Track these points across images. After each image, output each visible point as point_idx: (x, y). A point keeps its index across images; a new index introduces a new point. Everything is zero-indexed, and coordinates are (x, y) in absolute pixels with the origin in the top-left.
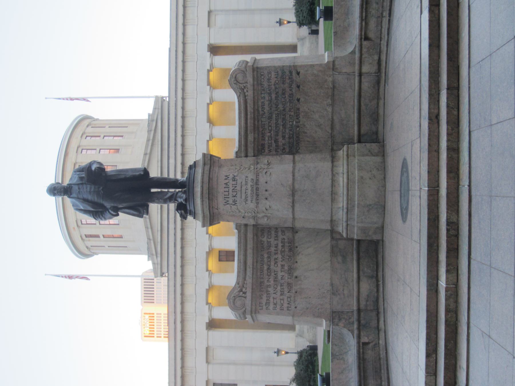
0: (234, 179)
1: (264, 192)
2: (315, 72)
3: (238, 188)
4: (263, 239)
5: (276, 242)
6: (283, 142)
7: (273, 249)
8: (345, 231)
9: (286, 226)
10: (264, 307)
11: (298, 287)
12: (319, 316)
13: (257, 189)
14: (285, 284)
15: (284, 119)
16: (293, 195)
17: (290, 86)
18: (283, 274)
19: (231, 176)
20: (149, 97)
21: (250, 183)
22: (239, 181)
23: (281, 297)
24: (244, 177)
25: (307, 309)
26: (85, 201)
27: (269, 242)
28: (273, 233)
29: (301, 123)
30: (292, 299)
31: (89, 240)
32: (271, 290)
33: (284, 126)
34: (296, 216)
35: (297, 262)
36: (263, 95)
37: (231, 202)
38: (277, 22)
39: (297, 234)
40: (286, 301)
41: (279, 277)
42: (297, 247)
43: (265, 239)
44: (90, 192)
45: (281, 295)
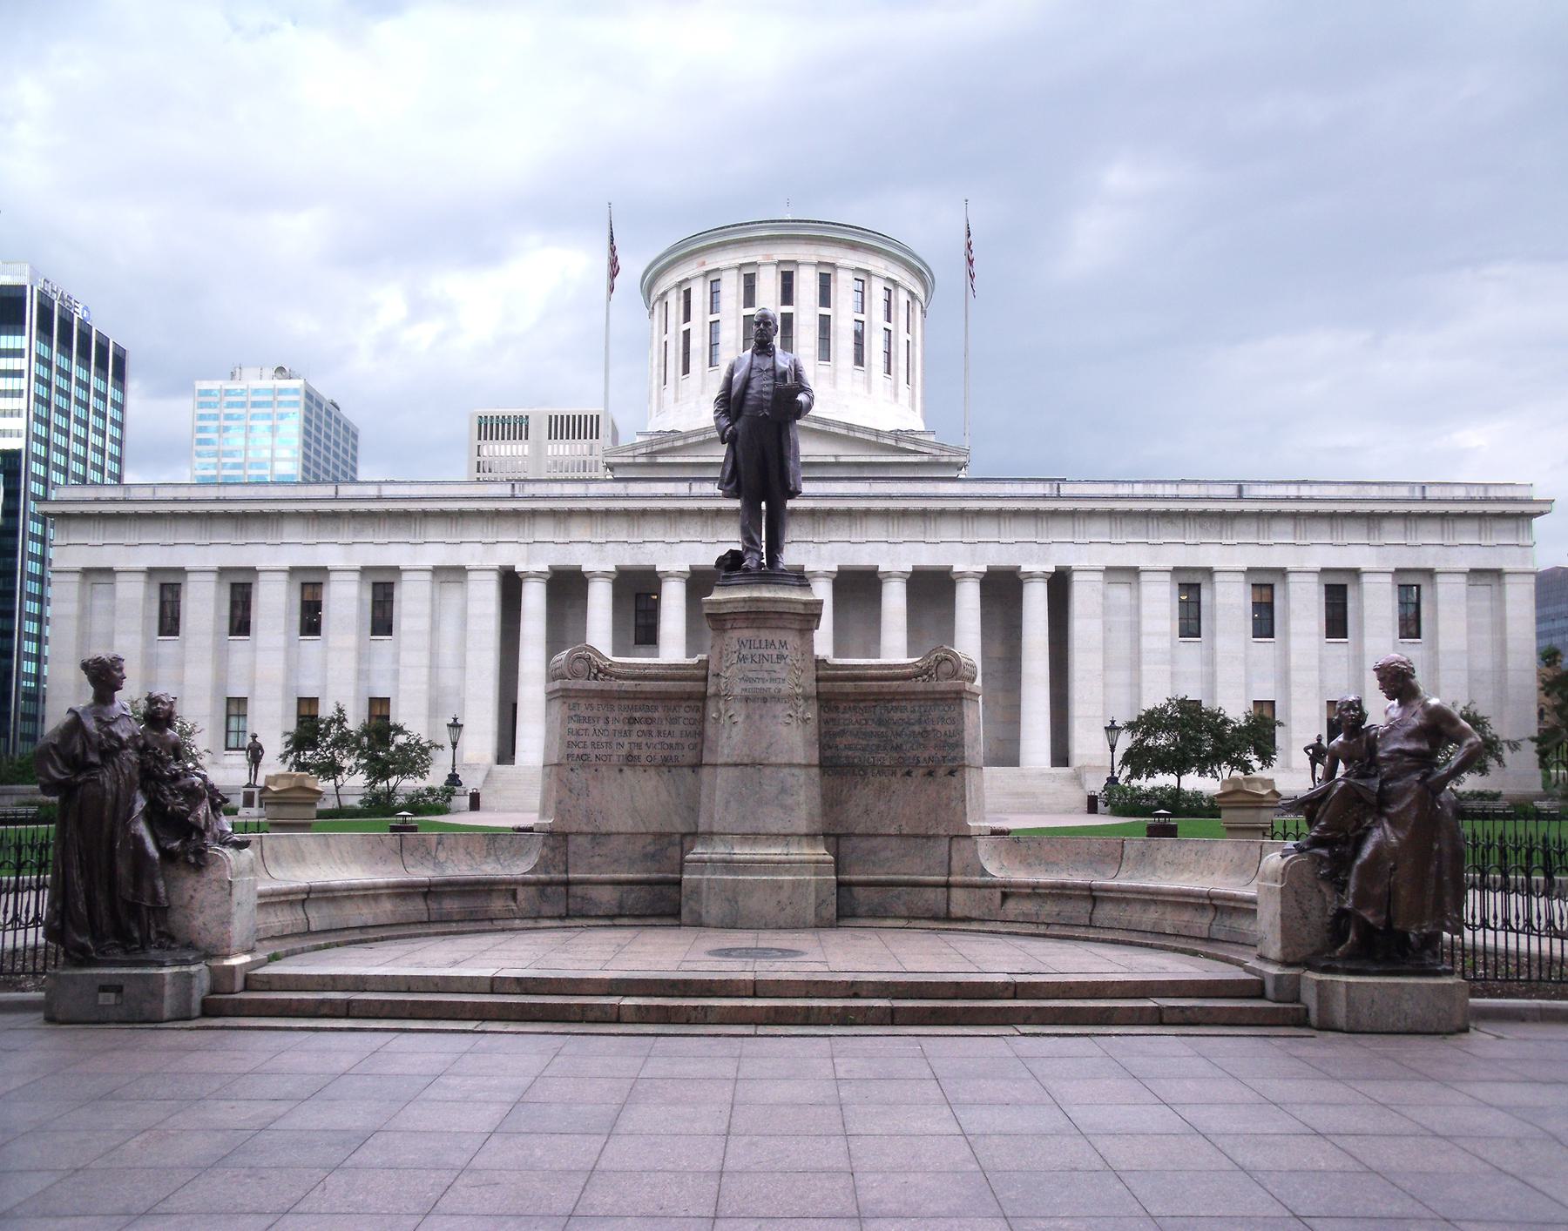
5: (677, 733)
9: (705, 752)
12: (560, 813)
16: (753, 765)
18: (627, 746)
26: (747, 382)
32: (600, 725)
34: (719, 770)
40: (581, 751)
43: (682, 713)
44: (761, 392)
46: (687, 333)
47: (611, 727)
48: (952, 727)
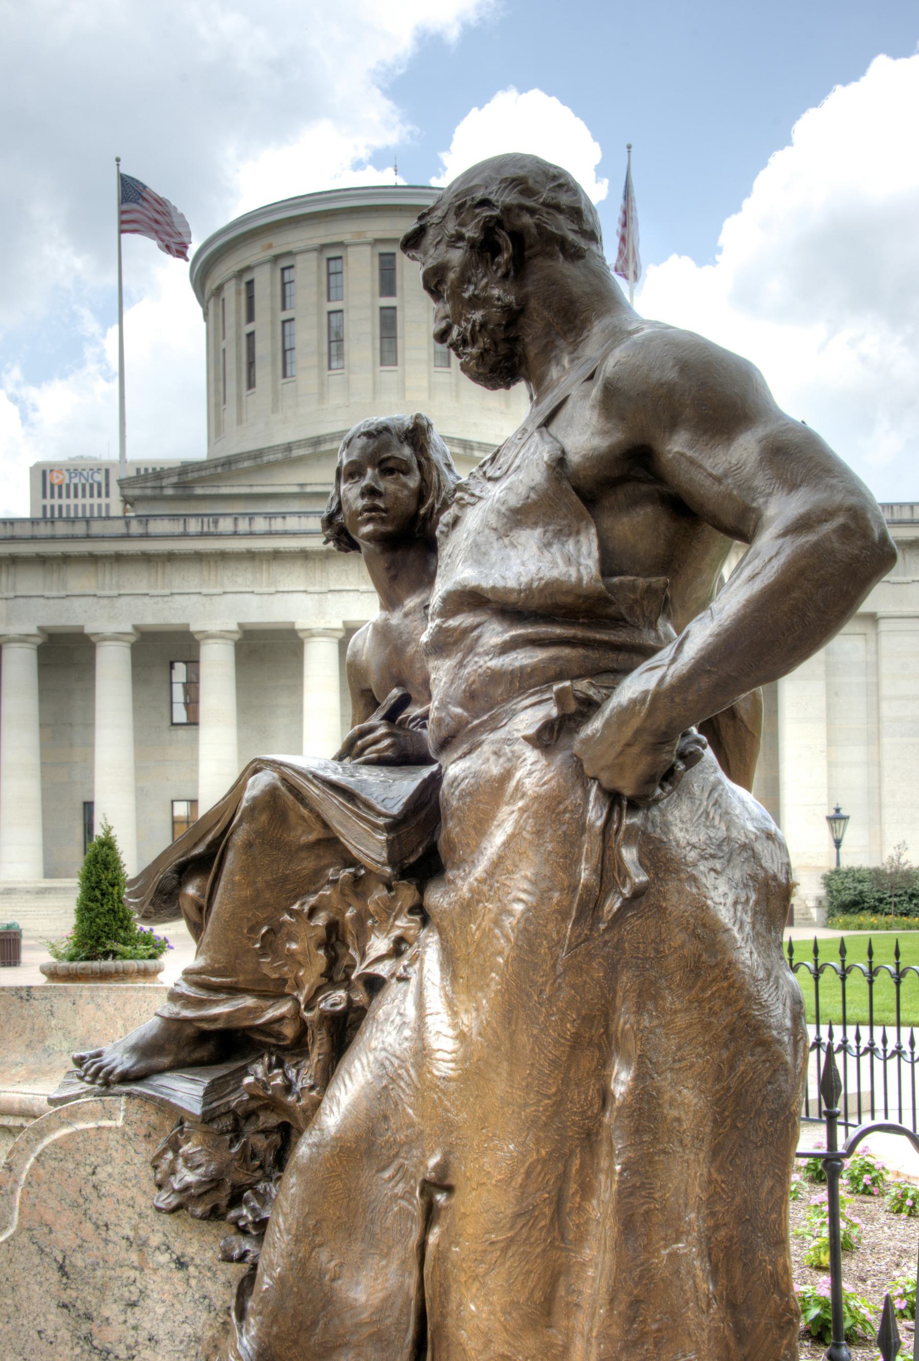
31: (238, 293)
38: (838, 810)
46: (251, 336)
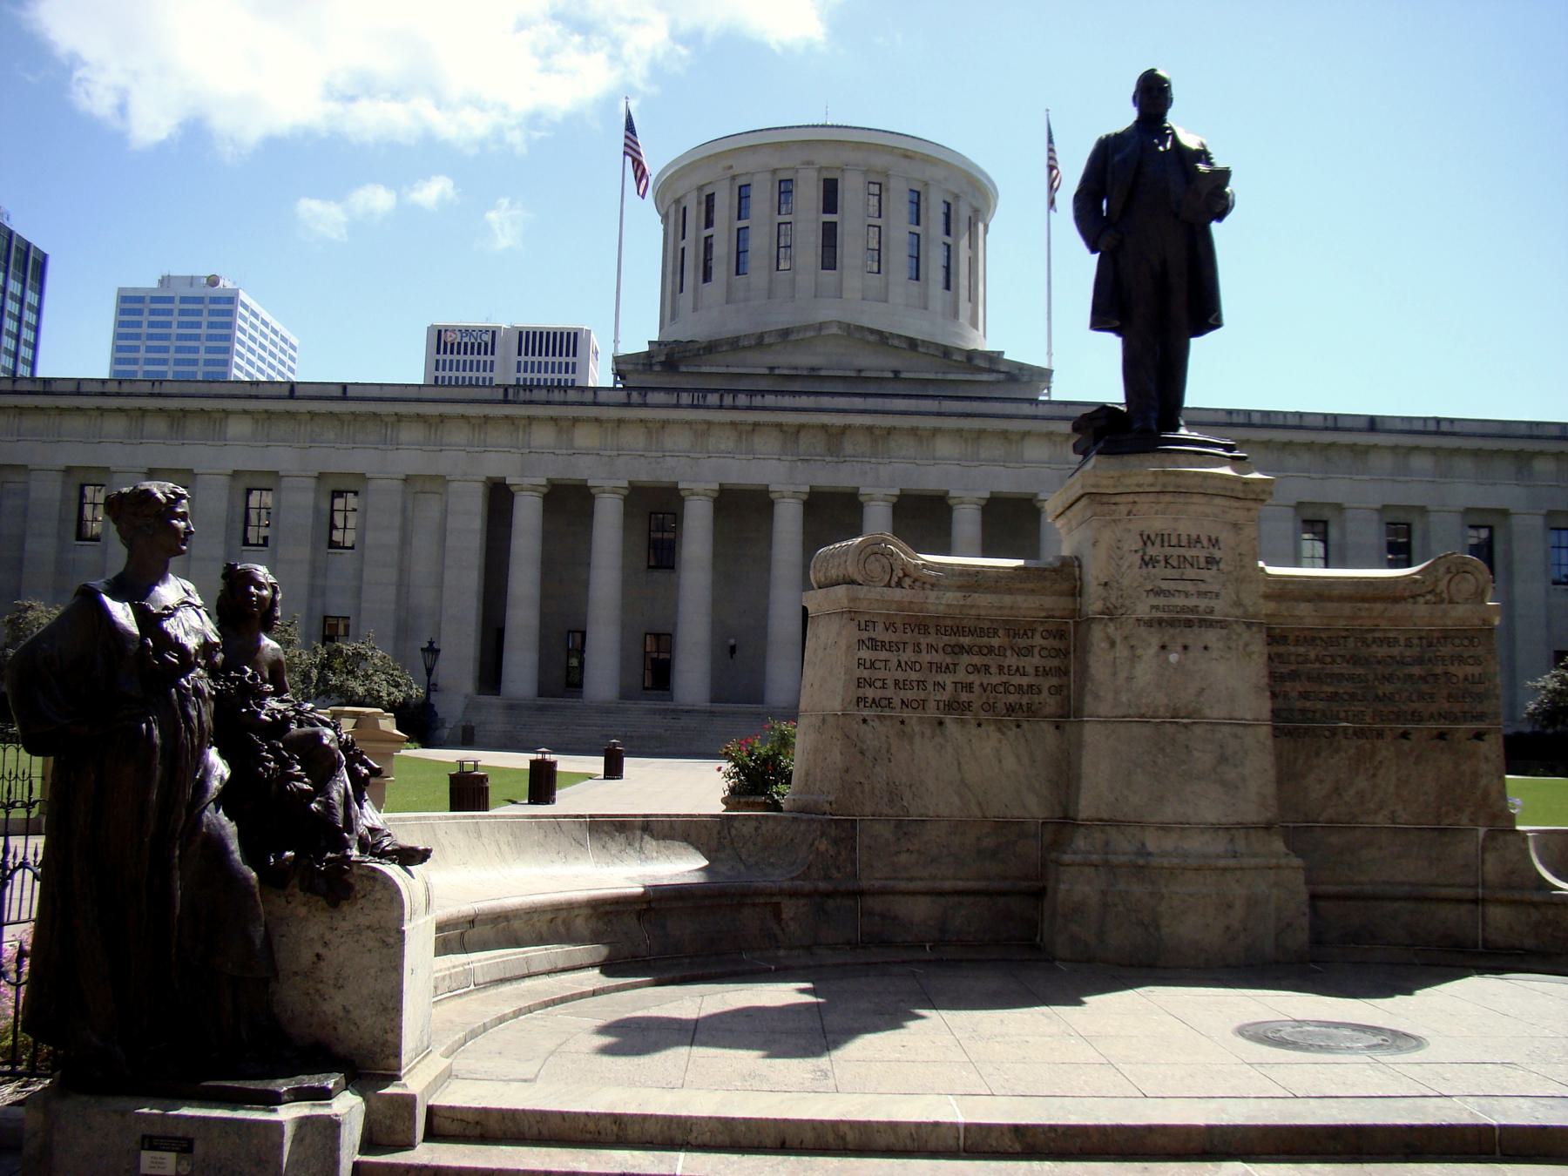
0: (1211, 561)
1: (1180, 641)
2: (1483, 782)
3: (1190, 573)
4: (1038, 636)
6: (1294, 694)
7: (1012, 660)
8: (1079, 858)
9: (1088, 699)
10: (865, 635)
11: (917, 729)
13: (1189, 624)
14: (923, 695)
15: (1353, 696)
17: (1442, 716)
18: (950, 687)
19: (1217, 554)
20: (1050, 354)
21: (1203, 603)
22: (1205, 574)
23: (890, 683)
24: (1216, 588)
25: (862, 753)
27: (1029, 651)
28: (1056, 663)
29: (1344, 742)
30: (887, 713)
31: (699, 203)
32: (908, 655)
33: (1334, 697)
35: (979, 725)
36: (1416, 641)
37: (1152, 551)
39: (1052, 729)
40: (879, 694)
41: (940, 678)
42: (1018, 726)
43: (1038, 640)
45: (896, 683)
47: (926, 657)
48: (1476, 670)
